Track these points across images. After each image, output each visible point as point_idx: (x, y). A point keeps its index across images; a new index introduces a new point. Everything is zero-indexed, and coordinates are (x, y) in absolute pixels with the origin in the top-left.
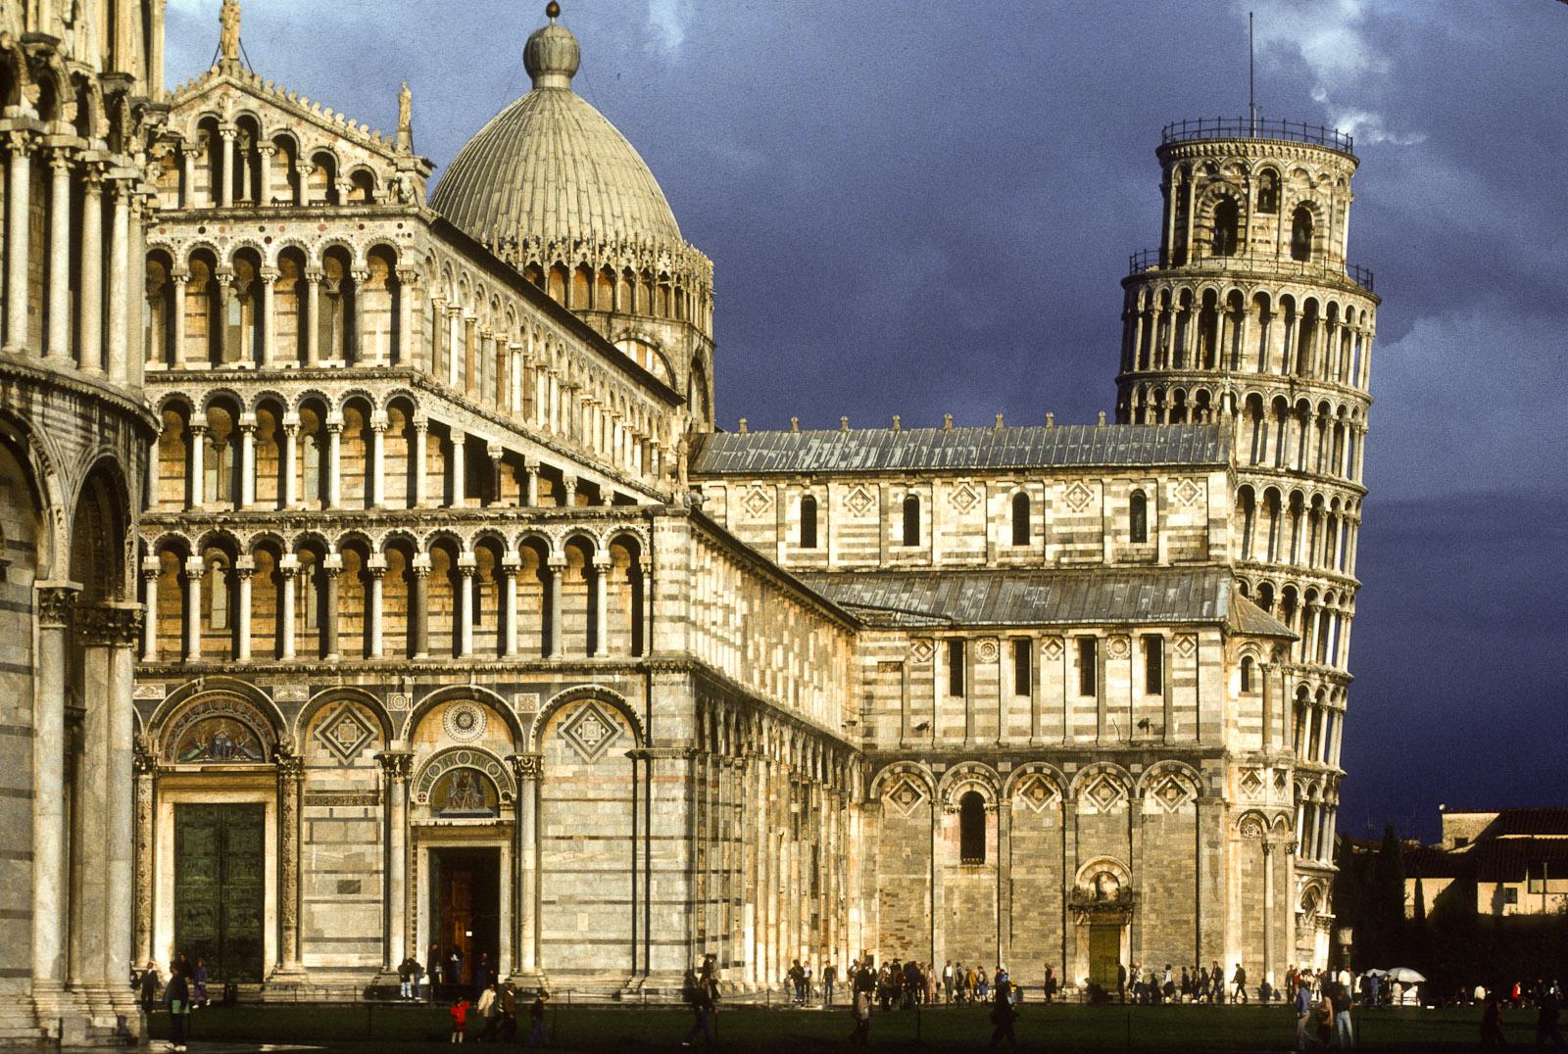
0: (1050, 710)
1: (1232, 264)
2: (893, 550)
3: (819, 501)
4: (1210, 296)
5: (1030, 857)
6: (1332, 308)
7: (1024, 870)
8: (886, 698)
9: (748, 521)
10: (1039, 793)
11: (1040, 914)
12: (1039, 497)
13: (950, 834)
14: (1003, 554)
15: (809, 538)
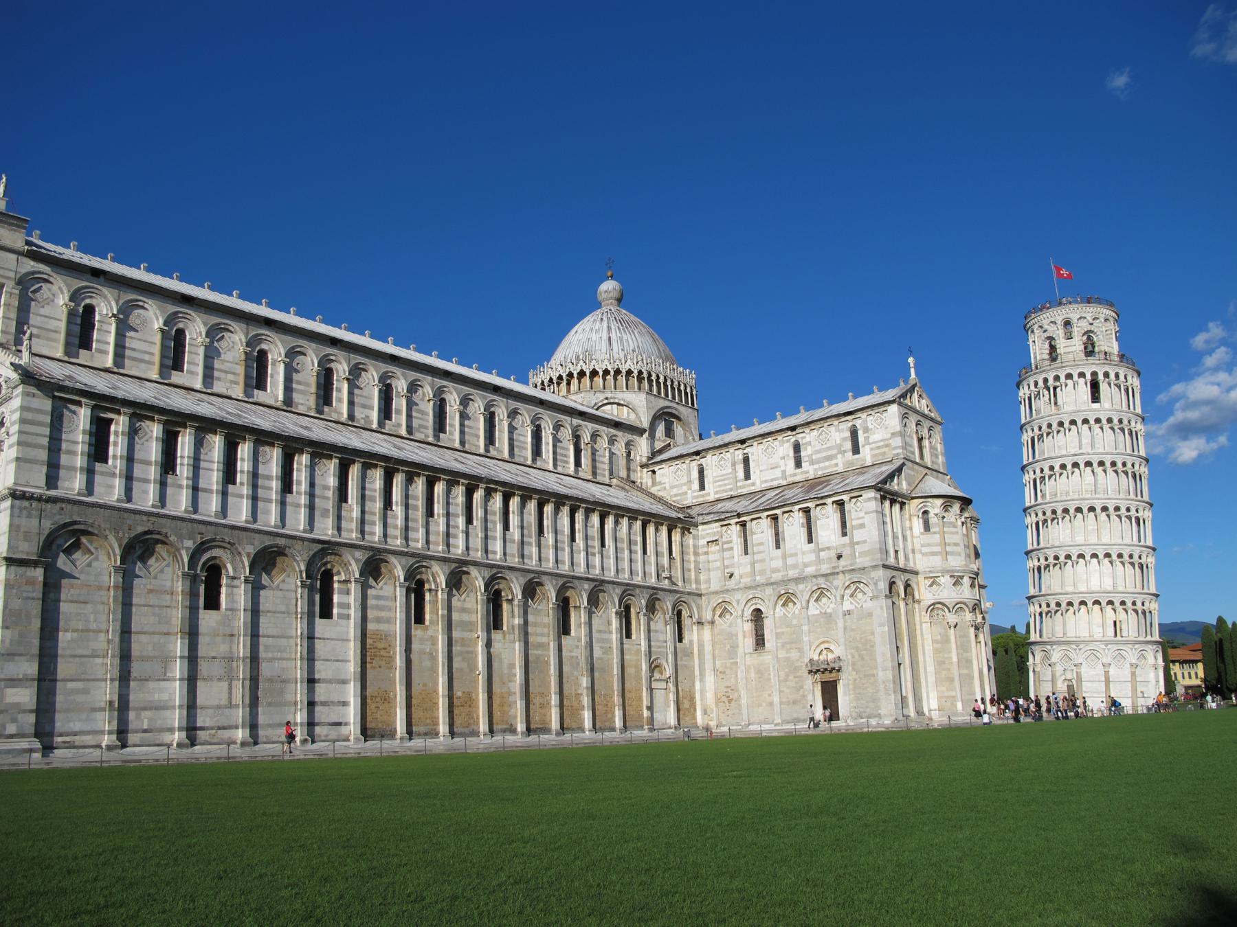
0: (791, 555)
1: (1055, 365)
2: (739, 484)
3: (704, 466)
4: (1046, 380)
5: (787, 643)
6: (1106, 375)
7: (784, 652)
8: (713, 561)
9: (677, 483)
10: (791, 605)
11: (795, 677)
12: (804, 441)
13: (747, 634)
14: (791, 476)
15: (702, 487)
